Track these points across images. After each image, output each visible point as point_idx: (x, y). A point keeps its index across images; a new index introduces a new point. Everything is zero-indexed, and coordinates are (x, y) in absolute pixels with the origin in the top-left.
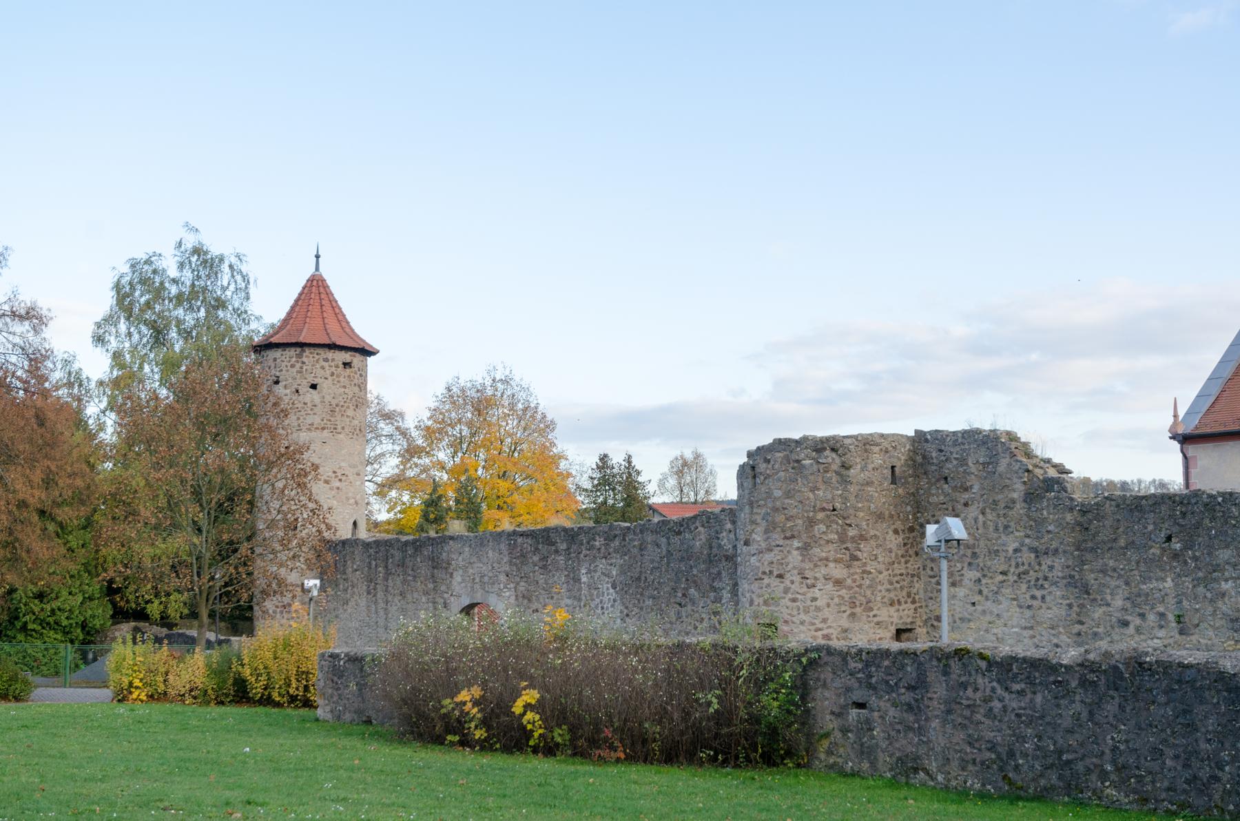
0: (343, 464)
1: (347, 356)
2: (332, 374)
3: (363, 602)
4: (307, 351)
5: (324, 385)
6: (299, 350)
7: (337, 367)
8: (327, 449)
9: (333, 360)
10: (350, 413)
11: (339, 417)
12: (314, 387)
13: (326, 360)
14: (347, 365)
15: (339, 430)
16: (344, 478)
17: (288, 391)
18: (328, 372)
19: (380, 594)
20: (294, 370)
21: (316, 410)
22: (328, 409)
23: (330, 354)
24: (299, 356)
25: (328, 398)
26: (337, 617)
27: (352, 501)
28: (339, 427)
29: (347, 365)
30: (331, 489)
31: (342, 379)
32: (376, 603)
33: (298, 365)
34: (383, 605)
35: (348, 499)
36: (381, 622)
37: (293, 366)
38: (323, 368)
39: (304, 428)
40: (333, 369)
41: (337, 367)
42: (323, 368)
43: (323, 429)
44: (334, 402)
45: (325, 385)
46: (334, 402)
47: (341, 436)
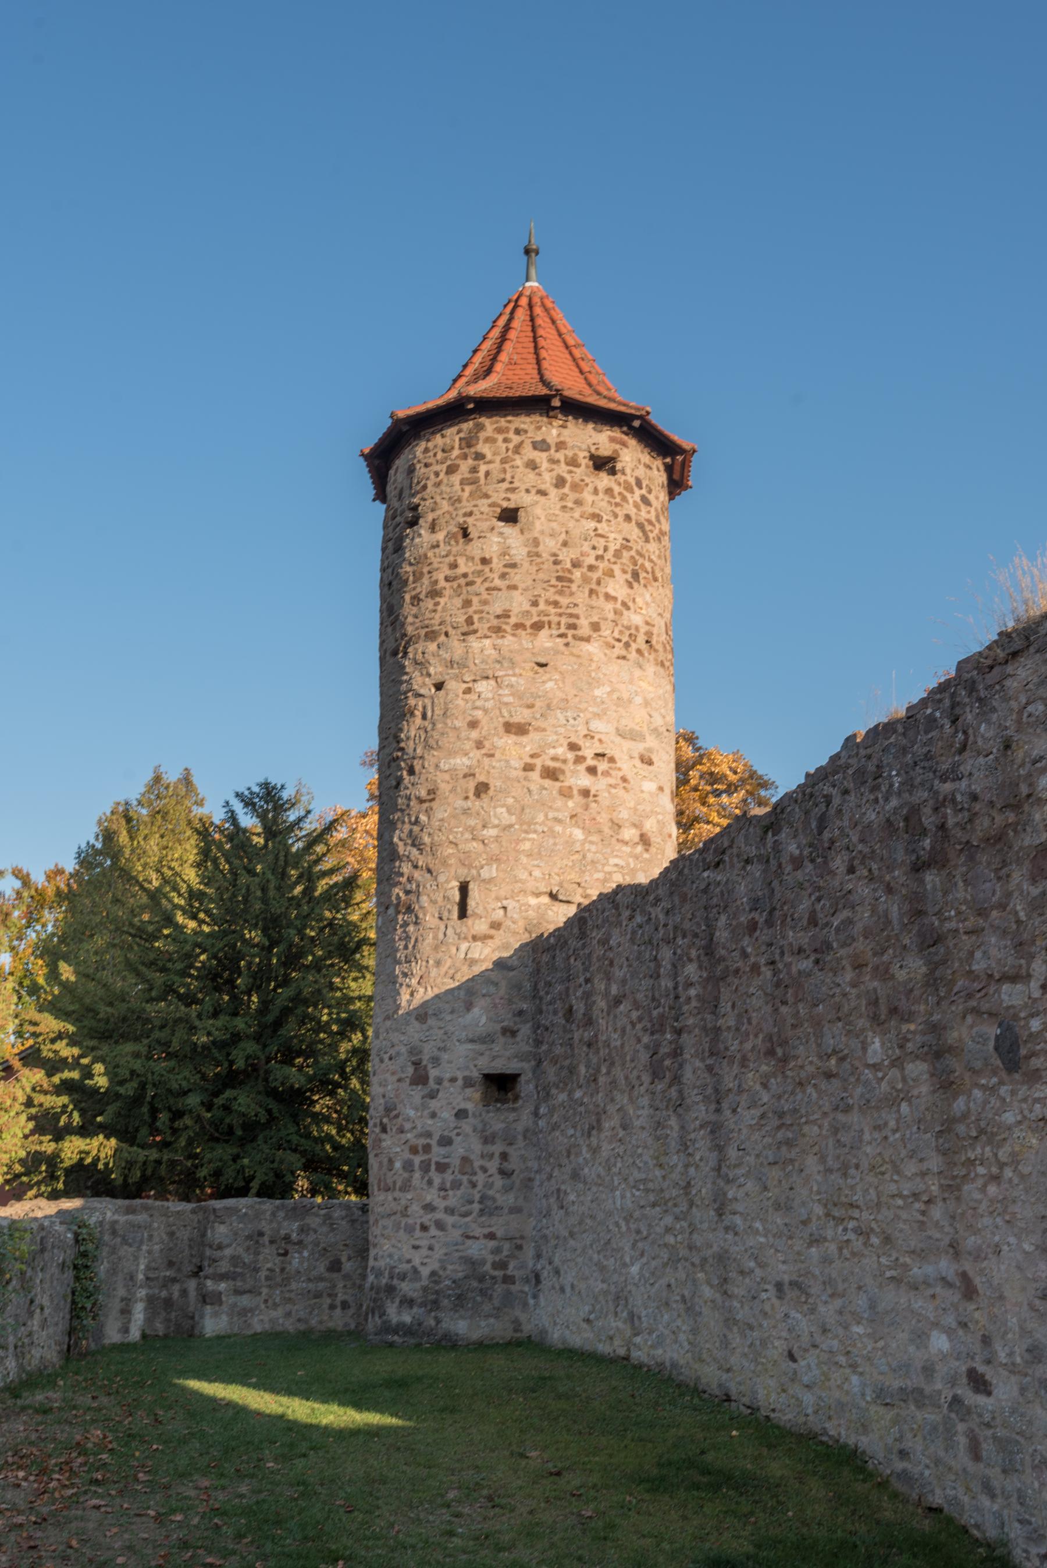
0: (597, 725)
1: (603, 439)
2: (560, 482)
3: (641, 1116)
4: (489, 424)
5: (542, 513)
6: (467, 426)
7: (573, 462)
8: (550, 684)
9: (561, 445)
10: (617, 587)
11: (581, 597)
12: (510, 516)
13: (541, 446)
14: (603, 464)
15: (585, 630)
16: (602, 766)
17: (440, 536)
18: (547, 480)
19: (693, 1070)
20: (456, 479)
21: (516, 577)
22: (549, 572)
23: (552, 430)
24: (468, 442)
25: (549, 545)
26: (575, 1176)
27: (629, 833)
28: (584, 623)
29: (603, 464)
30: (566, 793)
31: (588, 496)
32: (680, 1105)
33: (465, 466)
34: (701, 1112)
35: (617, 826)
36: (704, 1190)
37: (451, 470)
38: (532, 465)
39: (482, 627)
40: (562, 469)
41: (573, 462)
42: (532, 465)
43: (538, 626)
44: (566, 556)
45: (538, 511)
46: (566, 556)
47: (592, 648)
